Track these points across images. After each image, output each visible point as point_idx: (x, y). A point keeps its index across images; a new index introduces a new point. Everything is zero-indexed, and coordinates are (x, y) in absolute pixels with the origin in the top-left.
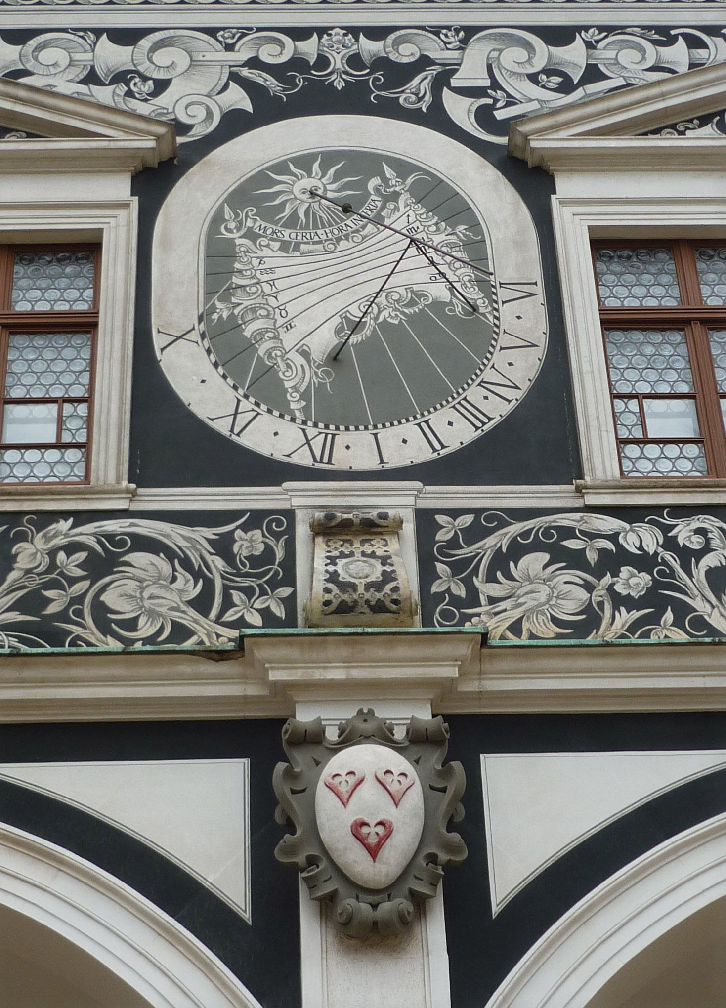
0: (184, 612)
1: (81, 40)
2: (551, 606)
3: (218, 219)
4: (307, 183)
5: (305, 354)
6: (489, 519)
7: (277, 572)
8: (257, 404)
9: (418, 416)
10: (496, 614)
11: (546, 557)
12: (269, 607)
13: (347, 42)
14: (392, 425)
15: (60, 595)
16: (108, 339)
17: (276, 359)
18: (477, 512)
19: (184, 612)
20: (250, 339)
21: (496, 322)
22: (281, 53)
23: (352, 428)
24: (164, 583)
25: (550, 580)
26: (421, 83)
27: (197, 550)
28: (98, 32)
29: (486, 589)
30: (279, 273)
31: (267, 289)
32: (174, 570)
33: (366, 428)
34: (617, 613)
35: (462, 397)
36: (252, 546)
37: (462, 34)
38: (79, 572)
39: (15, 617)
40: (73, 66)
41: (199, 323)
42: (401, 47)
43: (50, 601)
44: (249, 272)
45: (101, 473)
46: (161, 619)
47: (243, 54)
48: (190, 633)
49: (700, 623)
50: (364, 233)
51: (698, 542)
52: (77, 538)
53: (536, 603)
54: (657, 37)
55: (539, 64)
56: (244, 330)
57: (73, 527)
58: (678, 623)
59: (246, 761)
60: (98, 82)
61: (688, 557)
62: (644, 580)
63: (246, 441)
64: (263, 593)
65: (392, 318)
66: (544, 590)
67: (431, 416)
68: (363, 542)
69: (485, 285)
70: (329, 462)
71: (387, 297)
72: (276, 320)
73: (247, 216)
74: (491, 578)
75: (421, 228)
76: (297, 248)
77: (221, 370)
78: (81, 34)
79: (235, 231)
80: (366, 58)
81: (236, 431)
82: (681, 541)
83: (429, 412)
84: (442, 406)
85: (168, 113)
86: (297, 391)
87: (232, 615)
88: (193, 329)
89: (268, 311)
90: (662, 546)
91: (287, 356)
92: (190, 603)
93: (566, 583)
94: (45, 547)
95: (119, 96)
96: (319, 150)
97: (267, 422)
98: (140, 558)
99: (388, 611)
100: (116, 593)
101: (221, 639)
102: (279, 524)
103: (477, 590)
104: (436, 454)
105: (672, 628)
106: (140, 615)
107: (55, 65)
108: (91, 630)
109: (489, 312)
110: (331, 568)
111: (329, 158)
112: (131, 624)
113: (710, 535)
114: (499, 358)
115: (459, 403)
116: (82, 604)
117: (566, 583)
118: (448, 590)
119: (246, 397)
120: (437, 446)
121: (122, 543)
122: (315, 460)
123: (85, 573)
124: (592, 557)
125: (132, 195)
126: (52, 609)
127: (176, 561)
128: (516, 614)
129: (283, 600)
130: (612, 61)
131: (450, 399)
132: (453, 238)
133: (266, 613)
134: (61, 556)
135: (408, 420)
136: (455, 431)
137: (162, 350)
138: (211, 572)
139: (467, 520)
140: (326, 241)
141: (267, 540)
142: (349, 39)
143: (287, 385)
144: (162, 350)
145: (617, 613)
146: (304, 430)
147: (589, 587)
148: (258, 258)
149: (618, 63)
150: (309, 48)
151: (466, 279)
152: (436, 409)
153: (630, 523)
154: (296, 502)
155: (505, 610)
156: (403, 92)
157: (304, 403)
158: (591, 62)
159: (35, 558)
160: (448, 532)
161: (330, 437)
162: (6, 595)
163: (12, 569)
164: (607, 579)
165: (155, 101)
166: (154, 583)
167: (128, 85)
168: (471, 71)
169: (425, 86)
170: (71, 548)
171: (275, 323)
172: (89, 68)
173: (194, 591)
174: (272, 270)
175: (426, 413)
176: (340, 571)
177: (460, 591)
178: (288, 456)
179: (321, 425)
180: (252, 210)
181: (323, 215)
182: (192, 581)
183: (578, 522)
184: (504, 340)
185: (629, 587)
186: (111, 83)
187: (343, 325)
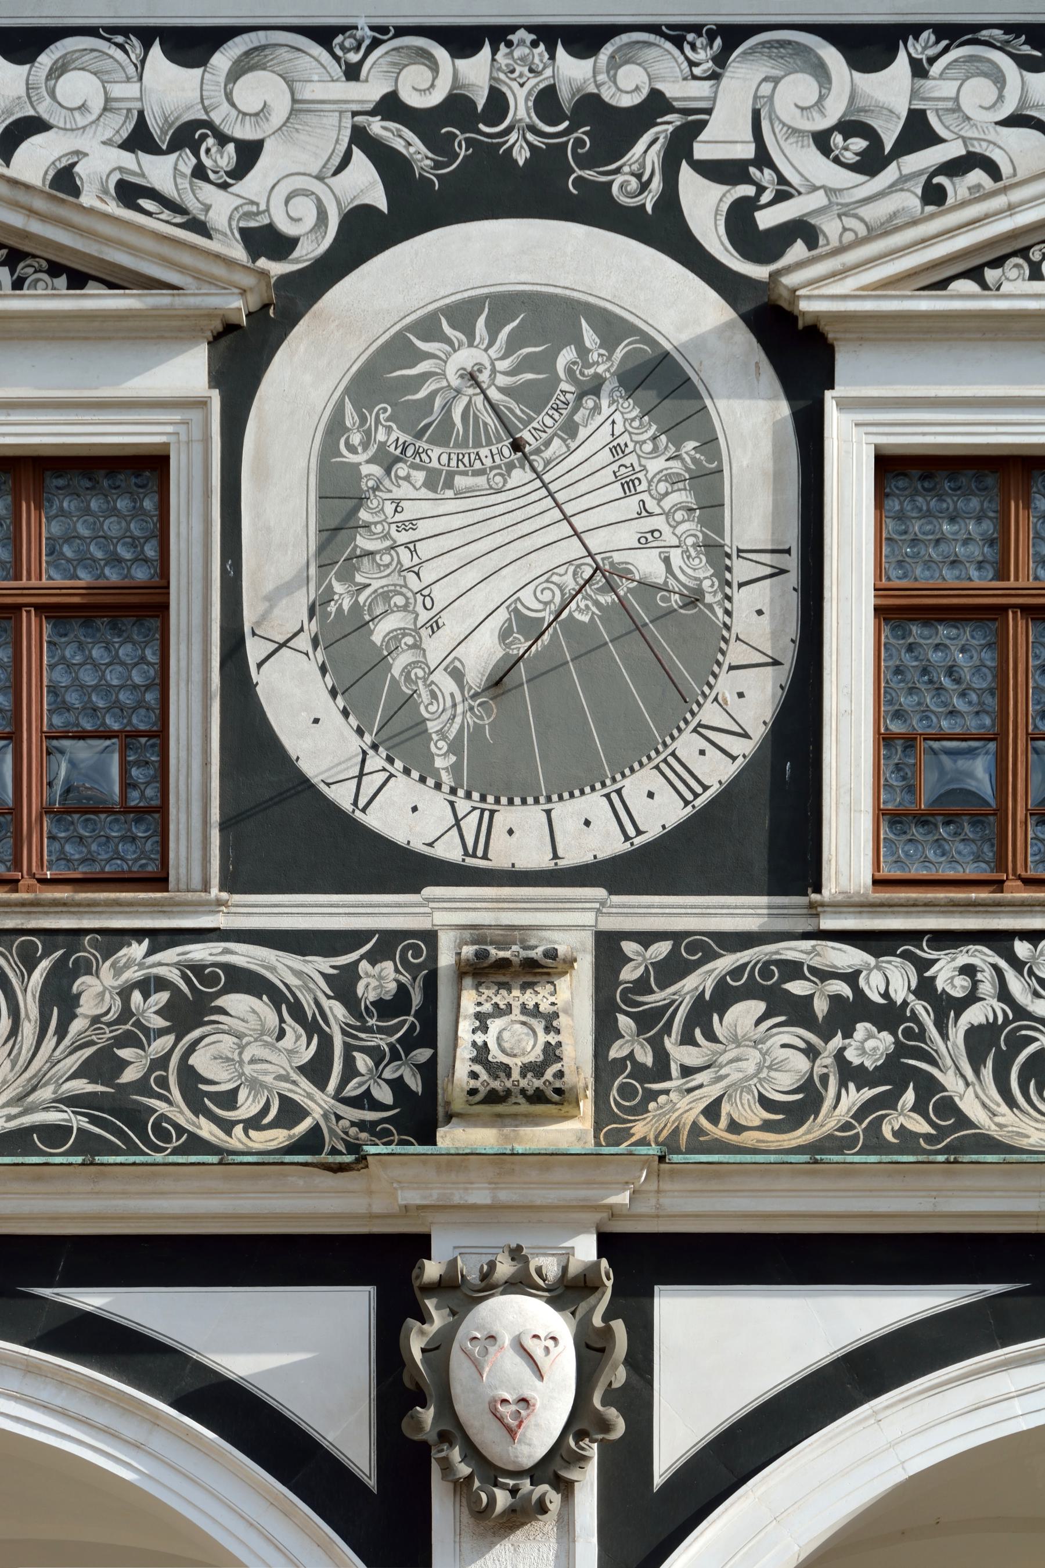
0: (294, 1083)
1: (119, 54)
2: (760, 1080)
3: (336, 427)
4: (466, 357)
5: (457, 675)
6: (691, 949)
7: (413, 1026)
8: (390, 760)
9: (608, 782)
10: (689, 1091)
11: (759, 1007)
12: (401, 1077)
13: (537, 60)
14: (572, 795)
15: (139, 1056)
16: (183, 647)
17: (416, 683)
18: (676, 937)
19: (294, 1083)
20: (381, 649)
21: (727, 620)
22: (432, 86)
23: (517, 800)
24: (268, 1039)
25: (763, 1041)
26: (646, 152)
27: (310, 990)
28: (147, 35)
29: (680, 1054)
30: (425, 528)
31: (404, 555)
32: (282, 1020)
33: (537, 801)
34: (843, 1091)
35: (669, 750)
36: (381, 986)
37: (718, 42)
38: (159, 1022)
39: (82, 1086)
40: (111, 110)
41: (310, 619)
42: (622, 72)
43: (124, 1064)
44: (379, 528)
45: (183, 871)
46: (266, 1093)
47: (371, 90)
48: (304, 1113)
49: (949, 1107)
50: (547, 454)
51: (963, 987)
52: (154, 971)
53: (741, 1075)
54: (1027, 50)
55: (834, 111)
56: (371, 632)
57: (150, 952)
58: (919, 1107)
59: (372, 1289)
60: (153, 149)
61: (946, 1008)
62: (884, 1042)
63: (374, 820)
64: (395, 1056)
65: (581, 611)
66: (754, 1056)
67: (626, 782)
68: (525, 987)
69: (715, 552)
70: (485, 857)
71: (575, 574)
72: (417, 615)
73: (377, 421)
74: (688, 1039)
75: (631, 445)
76: (449, 484)
77: (340, 702)
78: (120, 39)
79: (360, 449)
80: (565, 96)
81: (361, 804)
82: (940, 984)
83: (624, 776)
84: (641, 765)
85: (259, 213)
86: (444, 738)
87: (355, 1088)
88: (301, 630)
89: (407, 599)
90: (914, 993)
91: (432, 678)
92: (302, 1069)
93: (784, 1046)
94: (116, 984)
95: (183, 175)
96: (486, 291)
97: (403, 789)
98: (237, 1003)
99: (548, 1101)
100: (208, 1055)
101: (341, 1122)
102: (417, 954)
103: (667, 1055)
104: (628, 844)
105: (912, 1114)
106: (239, 1087)
107: (83, 108)
108: (178, 1107)
109: (720, 603)
110: (480, 1038)
111: (503, 306)
112: (229, 1100)
113: (979, 976)
114: (726, 684)
115: (665, 761)
116: (167, 1071)
117: (784, 1046)
118: (631, 1056)
119: (375, 747)
120: (631, 831)
121: (213, 980)
122: (466, 853)
123: (168, 1024)
124: (821, 1007)
125: (210, 387)
126: (129, 1075)
127: (284, 1007)
128: (713, 1092)
129: (419, 1067)
130: (950, 105)
131: (653, 754)
132: (676, 466)
133: (397, 1085)
134: (137, 996)
135: (593, 789)
136: (659, 809)
137: (259, 665)
138: (329, 1027)
139: (662, 949)
140: (492, 469)
141: (401, 978)
142: (541, 55)
143: (432, 726)
144: (259, 665)
145: (843, 1091)
146: (452, 804)
147: (811, 1052)
148: (393, 500)
149: (958, 109)
150: (476, 72)
151: (690, 541)
152: (632, 770)
153: (877, 955)
154: (441, 918)
155: (701, 1086)
156: (617, 171)
157: (453, 759)
158: (918, 105)
159: (103, 1000)
160: (636, 968)
161: (487, 814)
162: (71, 1053)
163: (75, 1016)
164: (837, 1041)
165: (239, 188)
166: (256, 1040)
167: (197, 155)
168: (724, 138)
169: (654, 158)
170: (148, 985)
171: (416, 619)
172: (136, 113)
173: (307, 1054)
174: (410, 524)
175: (618, 777)
176: (492, 1045)
177: (646, 1057)
178: (431, 845)
179: (476, 796)
180: (385, 410)
181: (489, 421)
182: (304, 1039)
183: (809, 953)
184: (736, 654)
185: (863, 1052)
186: (171, 150)
187: (510, 626)
